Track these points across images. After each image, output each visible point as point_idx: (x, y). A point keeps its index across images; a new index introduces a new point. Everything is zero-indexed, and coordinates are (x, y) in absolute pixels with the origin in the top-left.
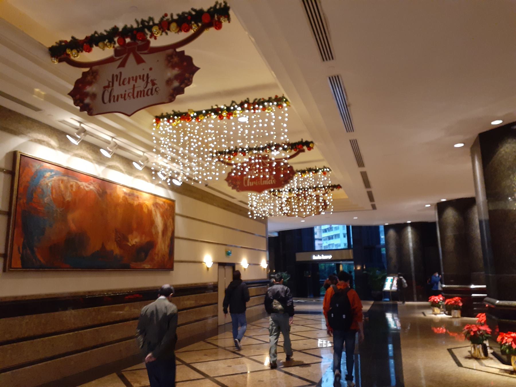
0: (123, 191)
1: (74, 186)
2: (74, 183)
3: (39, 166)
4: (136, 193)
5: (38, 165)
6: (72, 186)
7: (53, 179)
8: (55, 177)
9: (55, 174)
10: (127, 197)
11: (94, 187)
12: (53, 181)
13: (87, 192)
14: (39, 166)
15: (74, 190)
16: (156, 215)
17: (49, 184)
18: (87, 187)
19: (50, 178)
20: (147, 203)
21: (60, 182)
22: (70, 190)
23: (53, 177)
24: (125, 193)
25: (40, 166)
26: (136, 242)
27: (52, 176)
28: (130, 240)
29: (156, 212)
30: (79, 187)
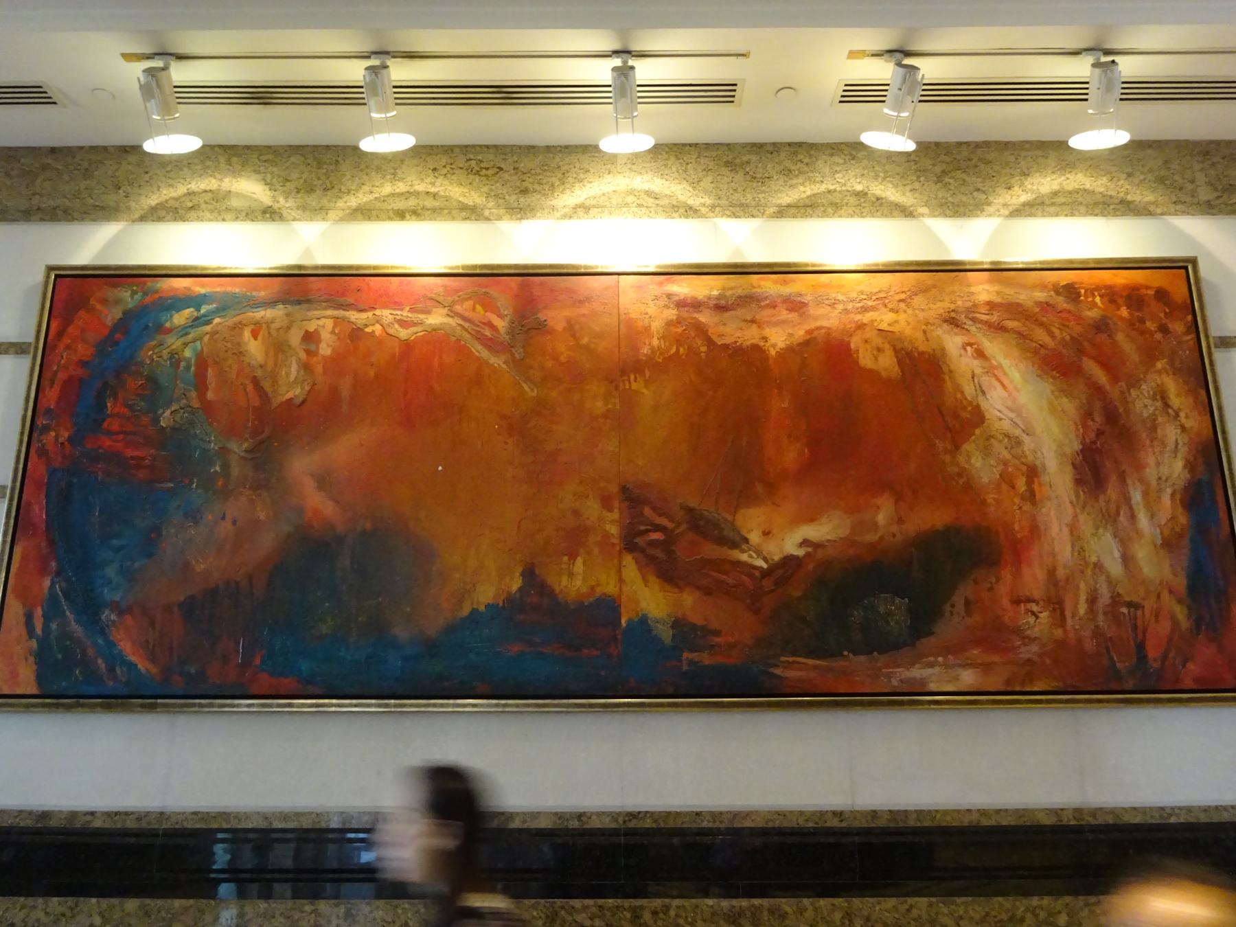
0: (669, 296)
1: (326, 336)
2: (329, 324)
3: (137, 297)
4: (769, 286)
5: (134, 293)
6: (310, 338)
7: (208, 328)
8: (217, 320)
9: (217, 312)
10: (704, 318)
11: (453, 314)
12: (206, 338)
13: (407, 346)
14: (137, 297)
15: (325, 350)
16: (992, 370)
17: (188, 353)
18: (404, 324)
19: (191, 327)
20: (885, 319)
21: (247, 334)
22: (303, 355)
23: (208, 322)
24: (696, 305)
25: (145, 294)
26: (805, 543)
27: (197, 322)
28: (754, 537)
29: (980, 354)
30: (356, 334)
